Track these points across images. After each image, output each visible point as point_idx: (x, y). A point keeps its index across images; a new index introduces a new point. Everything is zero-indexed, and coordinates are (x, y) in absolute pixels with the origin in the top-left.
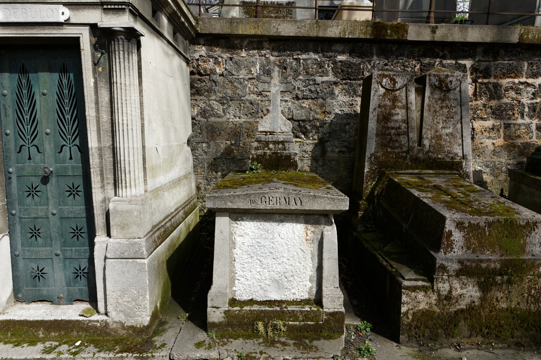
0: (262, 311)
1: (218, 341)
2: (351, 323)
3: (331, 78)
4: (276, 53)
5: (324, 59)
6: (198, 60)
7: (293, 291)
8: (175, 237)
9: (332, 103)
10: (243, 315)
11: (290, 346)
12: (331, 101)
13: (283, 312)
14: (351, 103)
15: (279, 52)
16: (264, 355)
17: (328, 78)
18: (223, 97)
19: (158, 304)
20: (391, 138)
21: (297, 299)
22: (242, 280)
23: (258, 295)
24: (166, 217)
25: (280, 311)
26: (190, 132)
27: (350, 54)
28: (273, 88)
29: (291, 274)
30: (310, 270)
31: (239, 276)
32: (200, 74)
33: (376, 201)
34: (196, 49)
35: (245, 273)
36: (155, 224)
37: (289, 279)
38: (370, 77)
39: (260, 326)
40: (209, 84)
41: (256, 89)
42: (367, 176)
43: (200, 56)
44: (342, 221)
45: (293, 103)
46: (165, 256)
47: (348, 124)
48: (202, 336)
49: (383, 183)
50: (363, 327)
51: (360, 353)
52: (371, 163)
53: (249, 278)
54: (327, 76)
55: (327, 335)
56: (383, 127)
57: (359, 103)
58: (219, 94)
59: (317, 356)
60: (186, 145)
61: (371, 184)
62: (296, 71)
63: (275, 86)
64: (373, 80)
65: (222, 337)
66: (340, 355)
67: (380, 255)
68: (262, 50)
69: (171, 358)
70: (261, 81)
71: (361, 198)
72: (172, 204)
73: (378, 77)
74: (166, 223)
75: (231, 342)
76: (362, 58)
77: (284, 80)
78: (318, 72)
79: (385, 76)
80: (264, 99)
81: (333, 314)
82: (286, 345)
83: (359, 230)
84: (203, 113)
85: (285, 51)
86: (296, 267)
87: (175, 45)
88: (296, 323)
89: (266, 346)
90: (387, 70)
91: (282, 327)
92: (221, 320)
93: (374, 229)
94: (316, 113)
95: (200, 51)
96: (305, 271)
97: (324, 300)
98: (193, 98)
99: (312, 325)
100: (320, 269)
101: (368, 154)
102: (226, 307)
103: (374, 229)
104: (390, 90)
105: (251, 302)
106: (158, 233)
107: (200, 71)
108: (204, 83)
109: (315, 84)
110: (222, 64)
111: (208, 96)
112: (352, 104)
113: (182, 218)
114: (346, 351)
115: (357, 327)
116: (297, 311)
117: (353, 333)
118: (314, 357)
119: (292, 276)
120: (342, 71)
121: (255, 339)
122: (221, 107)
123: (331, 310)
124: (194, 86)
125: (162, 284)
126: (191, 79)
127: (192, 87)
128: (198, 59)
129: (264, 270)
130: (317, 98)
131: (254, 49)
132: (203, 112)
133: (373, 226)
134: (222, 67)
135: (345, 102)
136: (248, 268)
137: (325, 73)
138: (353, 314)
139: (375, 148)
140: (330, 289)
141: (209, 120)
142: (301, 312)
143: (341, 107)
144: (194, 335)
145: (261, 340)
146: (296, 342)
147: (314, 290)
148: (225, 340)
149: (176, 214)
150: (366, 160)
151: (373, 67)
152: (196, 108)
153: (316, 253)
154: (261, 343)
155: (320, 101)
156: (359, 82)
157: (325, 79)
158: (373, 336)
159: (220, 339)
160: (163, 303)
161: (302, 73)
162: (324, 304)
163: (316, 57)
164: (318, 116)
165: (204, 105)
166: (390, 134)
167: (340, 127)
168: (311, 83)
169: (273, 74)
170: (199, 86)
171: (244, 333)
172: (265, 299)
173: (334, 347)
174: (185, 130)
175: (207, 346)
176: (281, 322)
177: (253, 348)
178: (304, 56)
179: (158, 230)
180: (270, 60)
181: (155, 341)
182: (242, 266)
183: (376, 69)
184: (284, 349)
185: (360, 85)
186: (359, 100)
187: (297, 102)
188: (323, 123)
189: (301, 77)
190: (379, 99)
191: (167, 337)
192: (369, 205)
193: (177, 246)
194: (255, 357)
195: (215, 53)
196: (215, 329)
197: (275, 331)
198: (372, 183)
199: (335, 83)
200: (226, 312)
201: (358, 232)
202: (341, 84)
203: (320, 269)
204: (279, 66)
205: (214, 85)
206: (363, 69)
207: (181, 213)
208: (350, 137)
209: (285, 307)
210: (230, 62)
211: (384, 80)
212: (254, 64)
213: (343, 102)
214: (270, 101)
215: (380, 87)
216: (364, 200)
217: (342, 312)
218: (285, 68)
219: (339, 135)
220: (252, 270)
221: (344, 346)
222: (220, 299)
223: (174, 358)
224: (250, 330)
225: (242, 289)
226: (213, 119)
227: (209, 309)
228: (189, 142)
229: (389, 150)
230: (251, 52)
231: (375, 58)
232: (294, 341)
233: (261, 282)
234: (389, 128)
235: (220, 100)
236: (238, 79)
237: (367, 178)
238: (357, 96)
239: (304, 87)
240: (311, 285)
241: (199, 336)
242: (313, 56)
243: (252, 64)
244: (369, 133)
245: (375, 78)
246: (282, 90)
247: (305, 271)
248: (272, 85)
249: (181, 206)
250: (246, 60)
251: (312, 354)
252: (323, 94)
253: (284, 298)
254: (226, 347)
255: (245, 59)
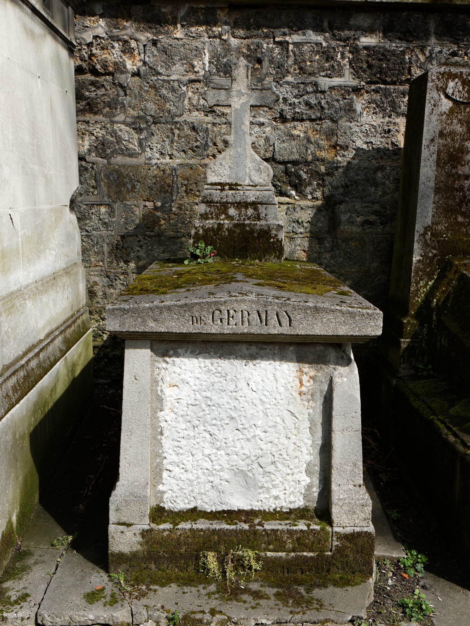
0: (214, 530)
1: (129, 589)
2: (387, 554)
3: (347, 79)
4: (241, 32)
5: (333, 43)
6: (90, 45)
7: (274, 492)
8: (47, 387)
9: (350, 128)
10: (178, 539)
11: (268, 598)
12: (348, 124)
13: (255, 533)
14: (386, 128)
15: (248, 29)
16: (218, 616)
17: (343, 79)
18: (138, 117)
19: (14, 519)
20: (465, 197)
21: (282, 507)
22: (176, 470)
23: (206, 500)
24: (30, 350)
25: (249, 531)
26: (75, 185)
27: (384, 34)
28: (236, 99)
29: (270, 459)
30: (306, 451)
31: (170, 463)
32: (94, 72)
33: (434, 317)
34: (87, 23)
35: (181, 457)
36: (7, 362)
37: (267, 470)
38: (424, 79)
39: (212, 560)
40: (112, 92)
41: (202, 102)
42: (418, 269)
43: (96, 37)
44: (371, 356)
45: (275, 128)
46: (26, 425)
47: (382, 168)
48: (98, 579)
49: (448, 284)
50: (409, 563)
51: (404, 612)
52: (426, 244)
53: (189, 467)
54: (341, 76)
55: (341, 578)
56: (449, 175)
57: (403, 129)
58: (132, 112)
59: (322, 618)
60: (68, 209)
61: (425, 286)
62: (280, 66)
63: (240, 96)
64: (430, 85)
65: (138, 581)
66: (365, 617)
67: (443, 422)
68: (215, 25)
69: (39, 622)
70: (212, 85)
71: (406, 313)
72: (41, 324)
73: (438, 78)
74: (29, 360)
75: (155, 591)
76: (407, 41)
77: (258, 84)
78: (322, 69)
79: (452, 76)
80: (218, 120)
81: (352, 538)
82: (262, 597)
83: (401, 375)
84: (101, 147)
85: (258, 28)
86: (280, 447)
87: (46, 16)
88: (280, 554)
89: (222, 598)
90: (456, 64)
91: (253, 563)
92: (135, 549)
93: (432, 372)
94: (320, 147)
95: (94, 28)
96: (298, 454)
97: (335, 510)
98: (81, 118)
99: (312, 558)
100: (326, 450)
101: (419, 228)
102: (145, 524)
103: (432, 372)
104: (463, 103)
105: (194, 514)
106: (14, 380)
107: (94, 67)
108: (103, 90)
109: (316, 92)
110: (136, 52)
111: (110, 116)
112: (389, 131)
113: (61, 350)
114: (376, 608)
115: (399, 561)
116: (283, 531)
117: (391, 574)
118: (315, 619)
119: (273, 463)
120: (370, 66)
121: (202, 586)
122: (136, 136)
123: (349, 530)
124: (83, 95)
125: (21, 478)
126: (77, 81)
127: (79, 97)
128: (91, 43)
129: (219, 453)
130: (320, 119)
131: (199, 24)
132: (100, 147)
133: (430, 367)
134: (138, 58)
135: (374, 127)
136: (188, 448)
137: (336, 71)
138: (391, 537)
139: (433, 216)
140: (345, 488)
141: (113, 160)
142: (290, 532)
143: (368, 135)
144: (83, 578)
145: (213, 588)
146: (281, 590)
147: (316, 491)
148: (144, 587)
149: (48, 344)
150: (416, 238)
151: (430, 59)
152: (87, 138)
153: (319, 419)
154: (213, 593)
155: (327, 124)
156: (401, 88)
157: (336, 81)
158: (428, 580)
159: (132, 585)
160: (22, 516)
161: (292, 70)
162: (335, 517)
163: (320, 39)
164: (323, 154)
165: (103, 132)
166: (461, 189)
167: (366, 175)
168: (310, 89)
169: (235, 73)
170: (93, 95)
171: (180, 573)
172: (220, 509)
173: (352, 601)
174: (67, 182)
175: (108, 599)
176: (251, 553)
177: (197, 602)
178: (296, 38)
179: (14, 373)
180: (229, 45)
181: (8, 589)
182: (176, 444)
183: (434, 62)
184: (258, 604)
185: (404, 94)
186: (402, 122)
187: (282, 127)
188: (333, 168)
189: (289, 78)
190: (441, 121)
191: (30, 581)
192: (421, 325)
193: (51, 404)
194: (201, 621)
195: (123, 32)
196: (124, 566)
197: (240, 569)
198: (427, 284)
199: (357, 90)
200: (144, 533)
201: (400, 378)
202: (367, 92)
203: (326, 450)
204: (247, 57)
205: (122, 93)
206: (410, 63)
207: (58, 342)
208: (385, 193)
209: (260, 524)
210: (153, 49)
211: (451, 84)
212: (199, 53)
213: (370, 127)
214: (230, 124)
215: (442, 97)
216: (412, 317)
217: (370, 533)
218: (259, 61)
219: (364, 190)
220: (194, 452)
221: (372, 599)
222: (134, 508)
223: (45, 622)
224: (191, 568)
225: (176, 488)
226: (119, 159)
227: (112, 528)
228: (73, 204)
229: (460, 219)
230: (193, 29)
231: (433, 40)
232: (275, 590)
233: (213, 475)
234: (459, 176)
235: (133, 123)
236: (168, 82)
237: (417, 273)
238: (398, 115)
239: (295, 97)
240: (308, 480)
241: (93, 579)
242: (313, 36)
243: (194, 52)
244: (421, 187)
245: (433, 81)
246: (252, 102)
247: (298, 454)
248: (234, 93)
249: (57, 328)
250: (183, 45)
251: (311, 615)
252: (332, 111)
253: (257, 506)
254: (144, 601)
255: (181, 42)
